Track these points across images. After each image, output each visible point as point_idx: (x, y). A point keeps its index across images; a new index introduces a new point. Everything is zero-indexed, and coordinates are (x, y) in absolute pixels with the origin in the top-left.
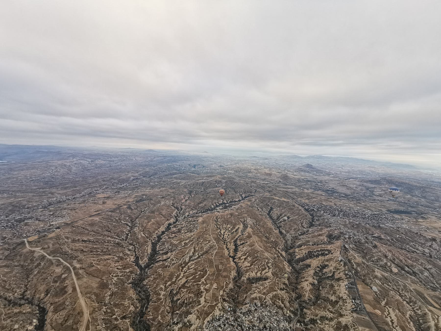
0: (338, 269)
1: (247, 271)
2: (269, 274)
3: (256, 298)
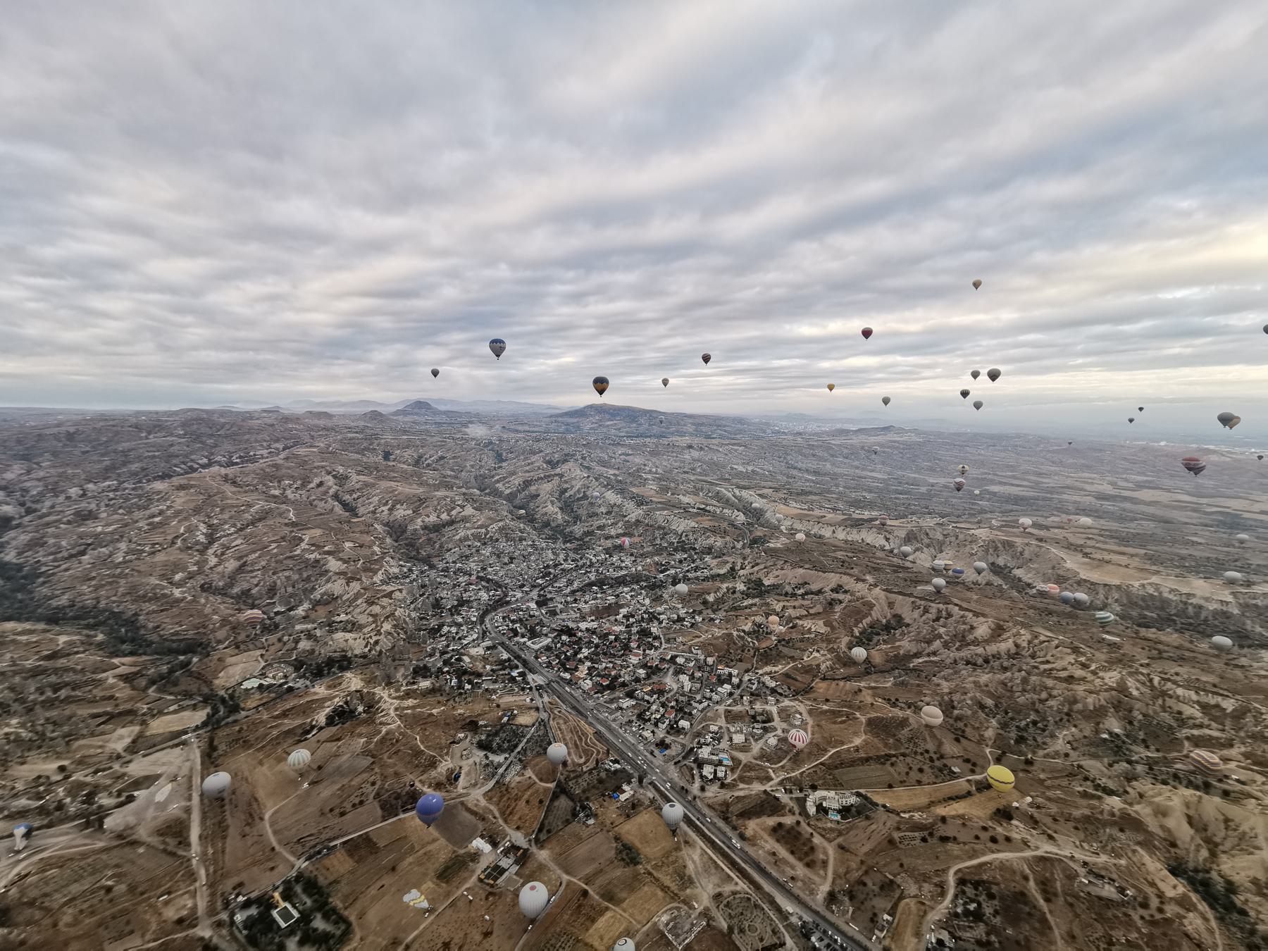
2: (469, 510)
3: (466, 538)
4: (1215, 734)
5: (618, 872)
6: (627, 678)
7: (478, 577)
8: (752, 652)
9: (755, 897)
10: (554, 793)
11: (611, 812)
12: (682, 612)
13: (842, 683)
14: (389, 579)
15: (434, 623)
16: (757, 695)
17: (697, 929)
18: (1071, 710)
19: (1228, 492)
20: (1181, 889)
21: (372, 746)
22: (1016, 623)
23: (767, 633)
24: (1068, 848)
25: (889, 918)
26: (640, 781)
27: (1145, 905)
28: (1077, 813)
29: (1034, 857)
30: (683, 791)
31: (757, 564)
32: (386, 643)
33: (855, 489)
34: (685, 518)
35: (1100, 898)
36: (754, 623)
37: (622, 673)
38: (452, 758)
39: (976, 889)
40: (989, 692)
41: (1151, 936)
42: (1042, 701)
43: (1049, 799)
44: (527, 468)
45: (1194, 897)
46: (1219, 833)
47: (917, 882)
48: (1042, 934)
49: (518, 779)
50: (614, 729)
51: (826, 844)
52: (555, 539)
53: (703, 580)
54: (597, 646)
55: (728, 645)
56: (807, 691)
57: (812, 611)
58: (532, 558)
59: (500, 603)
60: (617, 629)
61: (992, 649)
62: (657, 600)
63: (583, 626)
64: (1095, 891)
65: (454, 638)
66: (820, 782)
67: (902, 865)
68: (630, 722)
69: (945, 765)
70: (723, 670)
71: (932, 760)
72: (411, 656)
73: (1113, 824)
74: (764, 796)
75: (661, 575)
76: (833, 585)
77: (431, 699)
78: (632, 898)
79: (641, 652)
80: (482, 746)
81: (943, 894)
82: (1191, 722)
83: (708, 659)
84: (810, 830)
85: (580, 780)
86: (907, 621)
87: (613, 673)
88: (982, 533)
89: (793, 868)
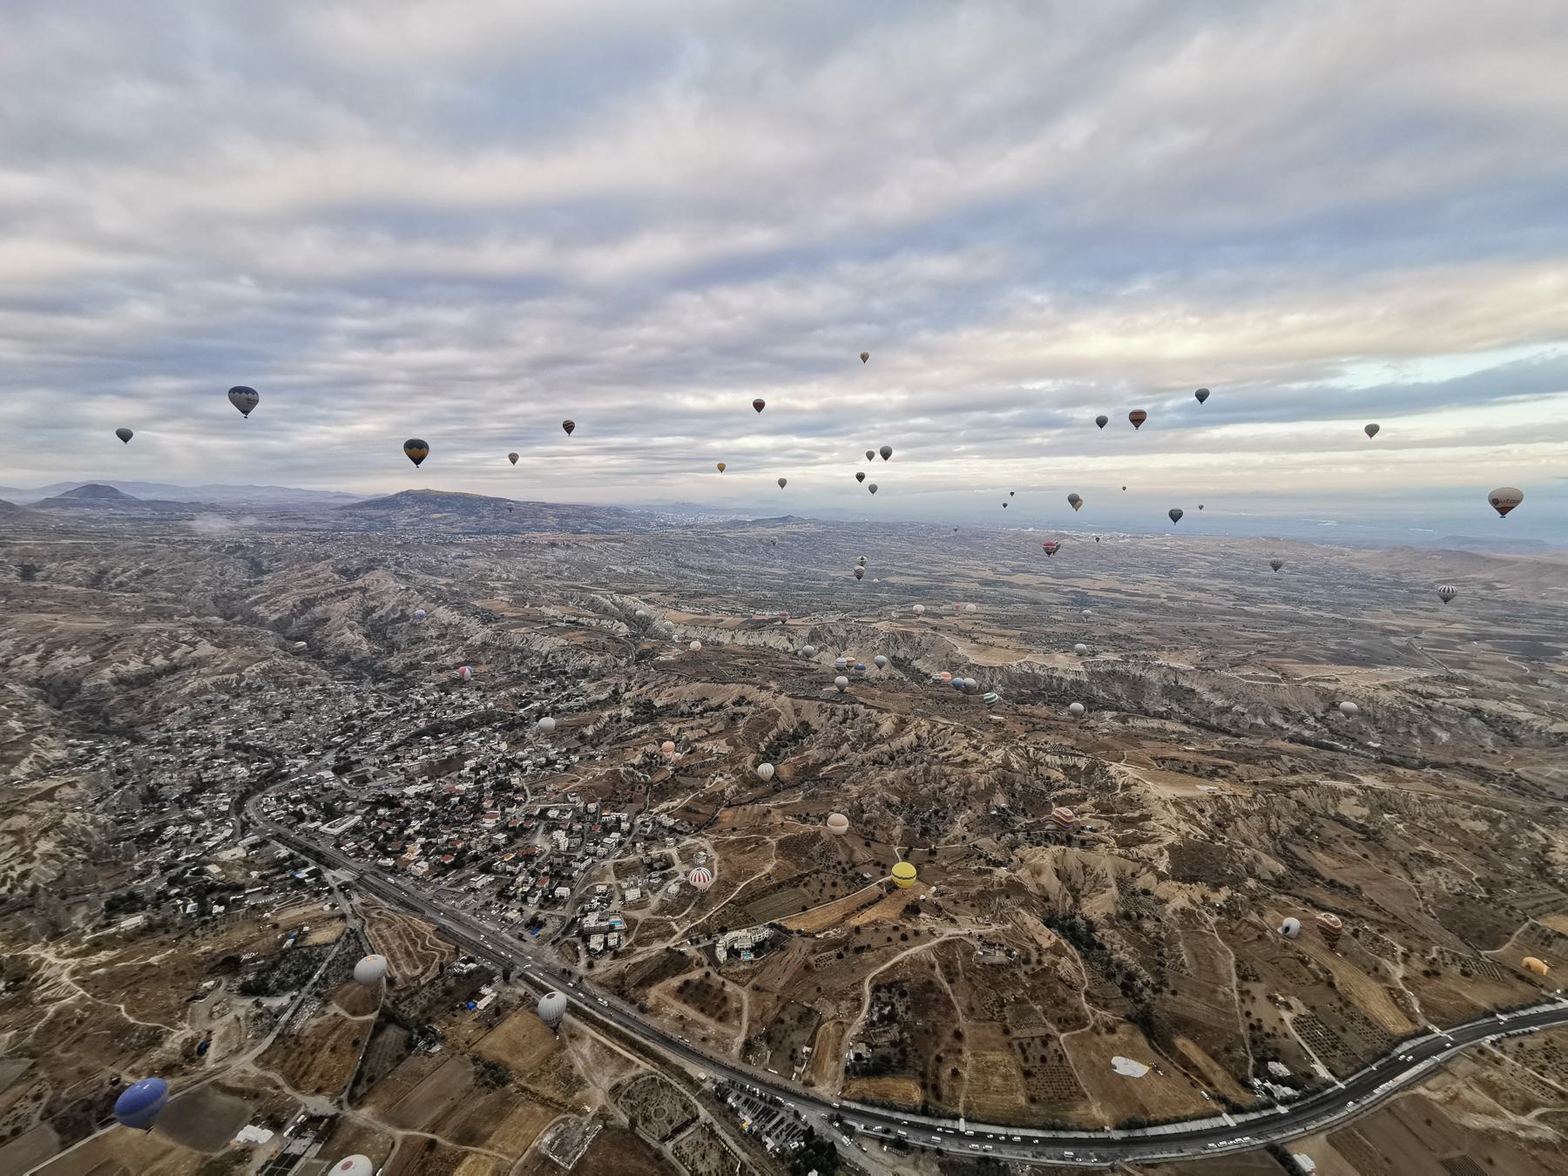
0: (408, 604)
1: (90, 672)
2: (205, 648)
3: (203, 690)
4: (1074, 791)
5: (480, 1102)
6: (480, 848)
7: (228, 746)
8: (644, 788)
9: (661, 1074)
10: (375, 1026)
11: (466, 1026)
12: (552, 753)
13: (749, 807)
14: (45, 770)
15: (146, 825)
16: (653, 839)
17: (589, 1138)
18: (966, 793)
19: (1079, 573)
20: (1054, 938)
21: (29, 1040)
22: (917, 715)
23: (661, 764)
24: (968, 927)
25: (808, 1049)
26: (506, 977)
27: (1027, 962)
28: (973, 891)
29: (939, 944)
30: (567, 974)
31: (646, 683)
32: (44, 873)
33: (754, 587)
34: (550, 635)
35: (992, 965)
36: (645, 754)
37: (472, 843)
38: (192, 1022)
39: (890, 992)
40: (896, 789)
41: (1033, 988)
42: (941, 790)
43: (951, 884)
44: (307, 581)
45: (1064, 943)
46: (1078, 878)
47: (835, 1002)
48: (947, 1015)
49: (315, 1022)
50: (465, 918)
51: (739, 989)
52: (359, 679)
53: (579, 710)
54: (433, 815)
55: (614, 785)
56: (711, 823)
57: (712, 730)
58: (323, 708)
59: (272, 777)
60: (462, 787)
61: (896, 744)
62: (518, 742)
63: (410, 791)
64: (988, 960)
65: (188, 842)
66: (730, 923)
67: (819, 989)
68: (488, 904)
69: (857, 874)
70: (609, 816)
71: (844, 871)
72: (100, 884)
73: (1000, 893)
74: (666, 955)
75: (522, 711)
76: (734, 698)
77: (146, 943)
78: (502, 1128)
79: (499, 812)
80: (246, 991)
81: (859, 1007)
82: (1057, 784)
83: (590, 806)
84: (721, 979)
85: (416, 999)
86: (814, 727)
87: (459, 846)
88: (883, 626)
89: (703, 1027)
